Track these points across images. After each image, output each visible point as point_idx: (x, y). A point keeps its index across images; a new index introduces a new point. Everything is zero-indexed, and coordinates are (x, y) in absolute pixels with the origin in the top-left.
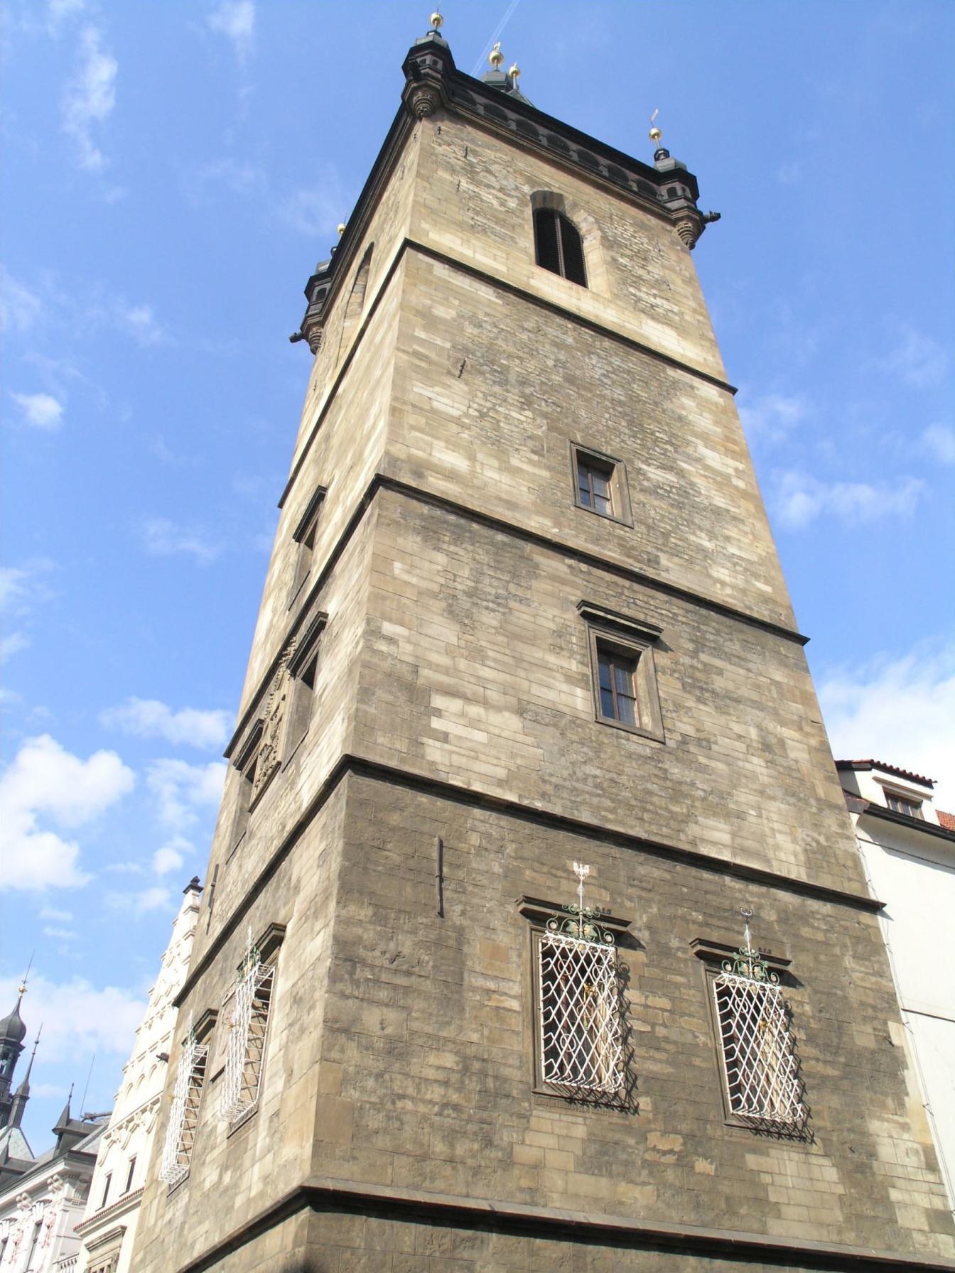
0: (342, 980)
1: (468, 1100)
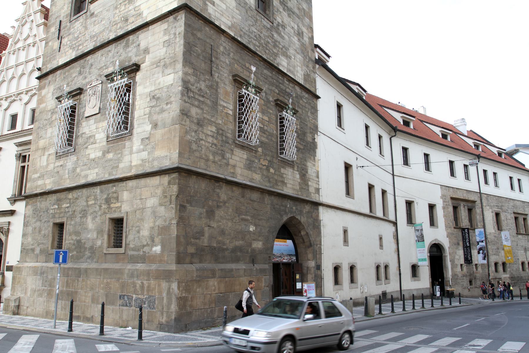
0: (185, 96)
1: (218, 143)
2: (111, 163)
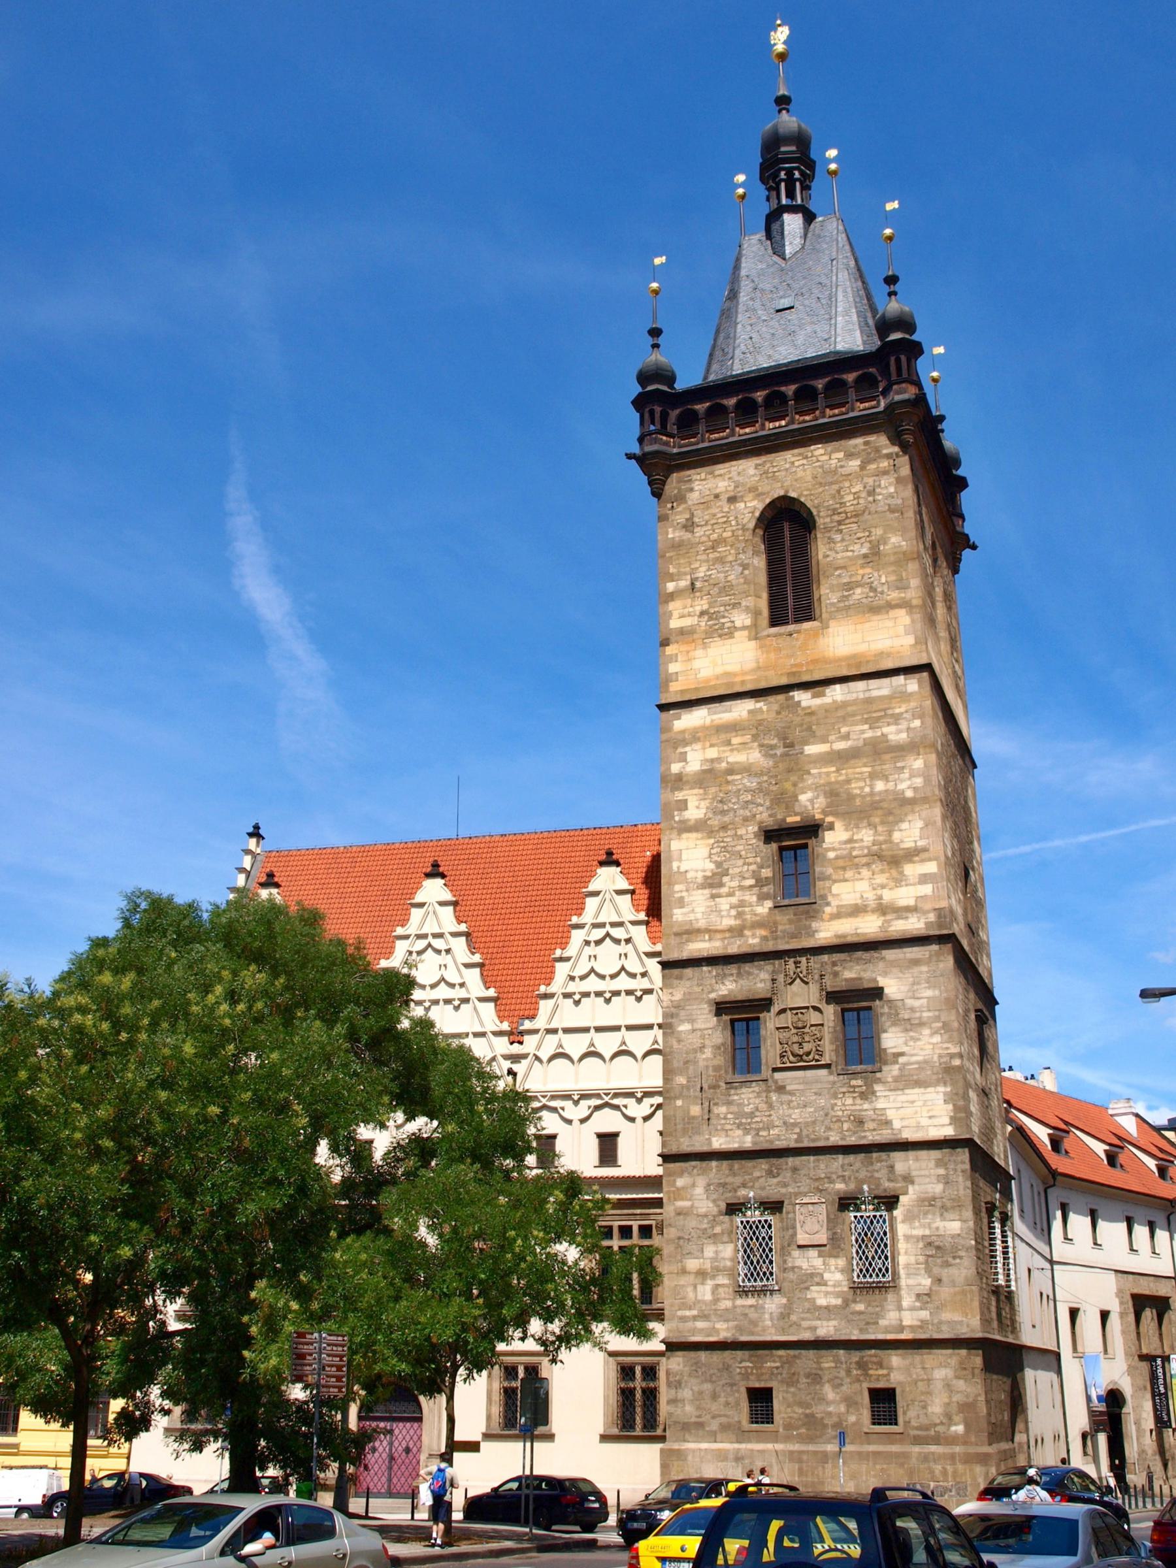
2: (862, 1317)
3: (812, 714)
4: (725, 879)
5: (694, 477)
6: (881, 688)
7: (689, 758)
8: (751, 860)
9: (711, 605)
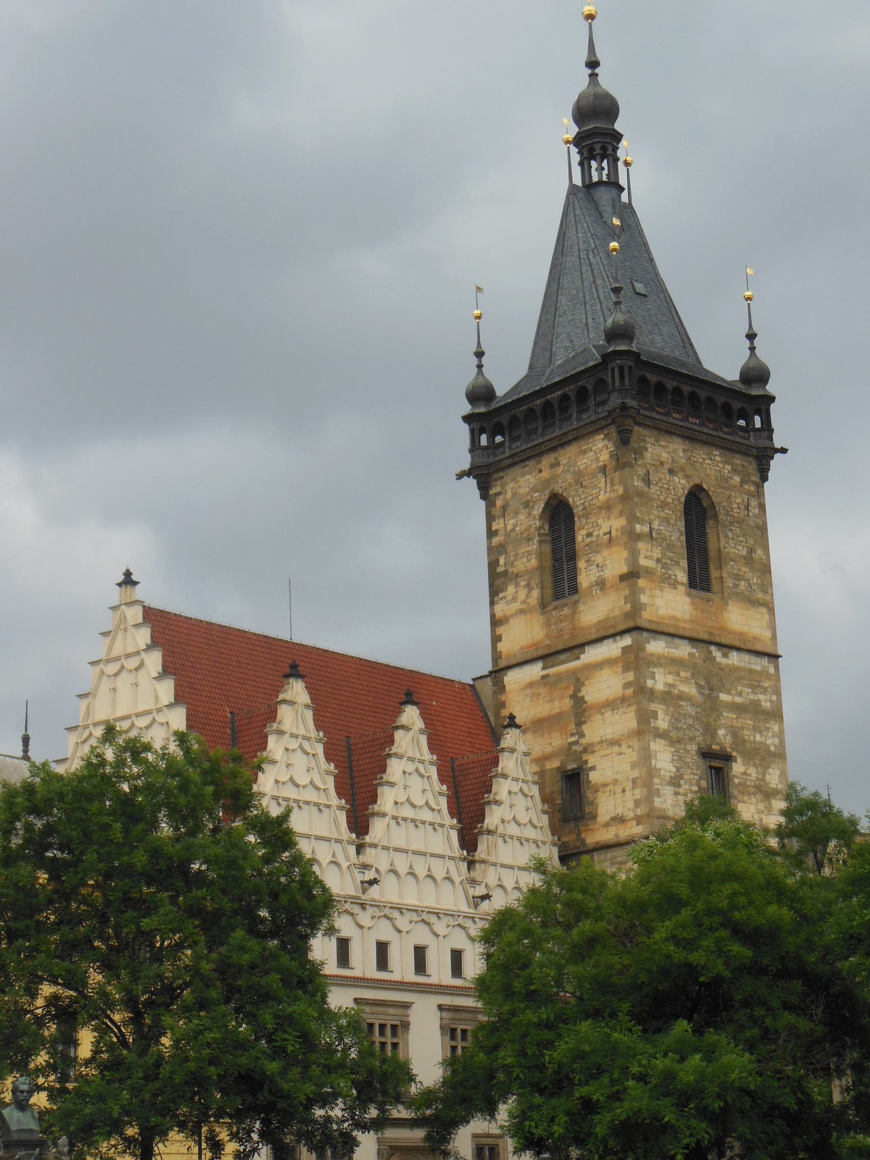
3: (722, 669)
4: (682, 782)
5: (648, 439)
6: (758, 664)
7: (657, 678)
8: (695, 771)
9: (663, 554)
